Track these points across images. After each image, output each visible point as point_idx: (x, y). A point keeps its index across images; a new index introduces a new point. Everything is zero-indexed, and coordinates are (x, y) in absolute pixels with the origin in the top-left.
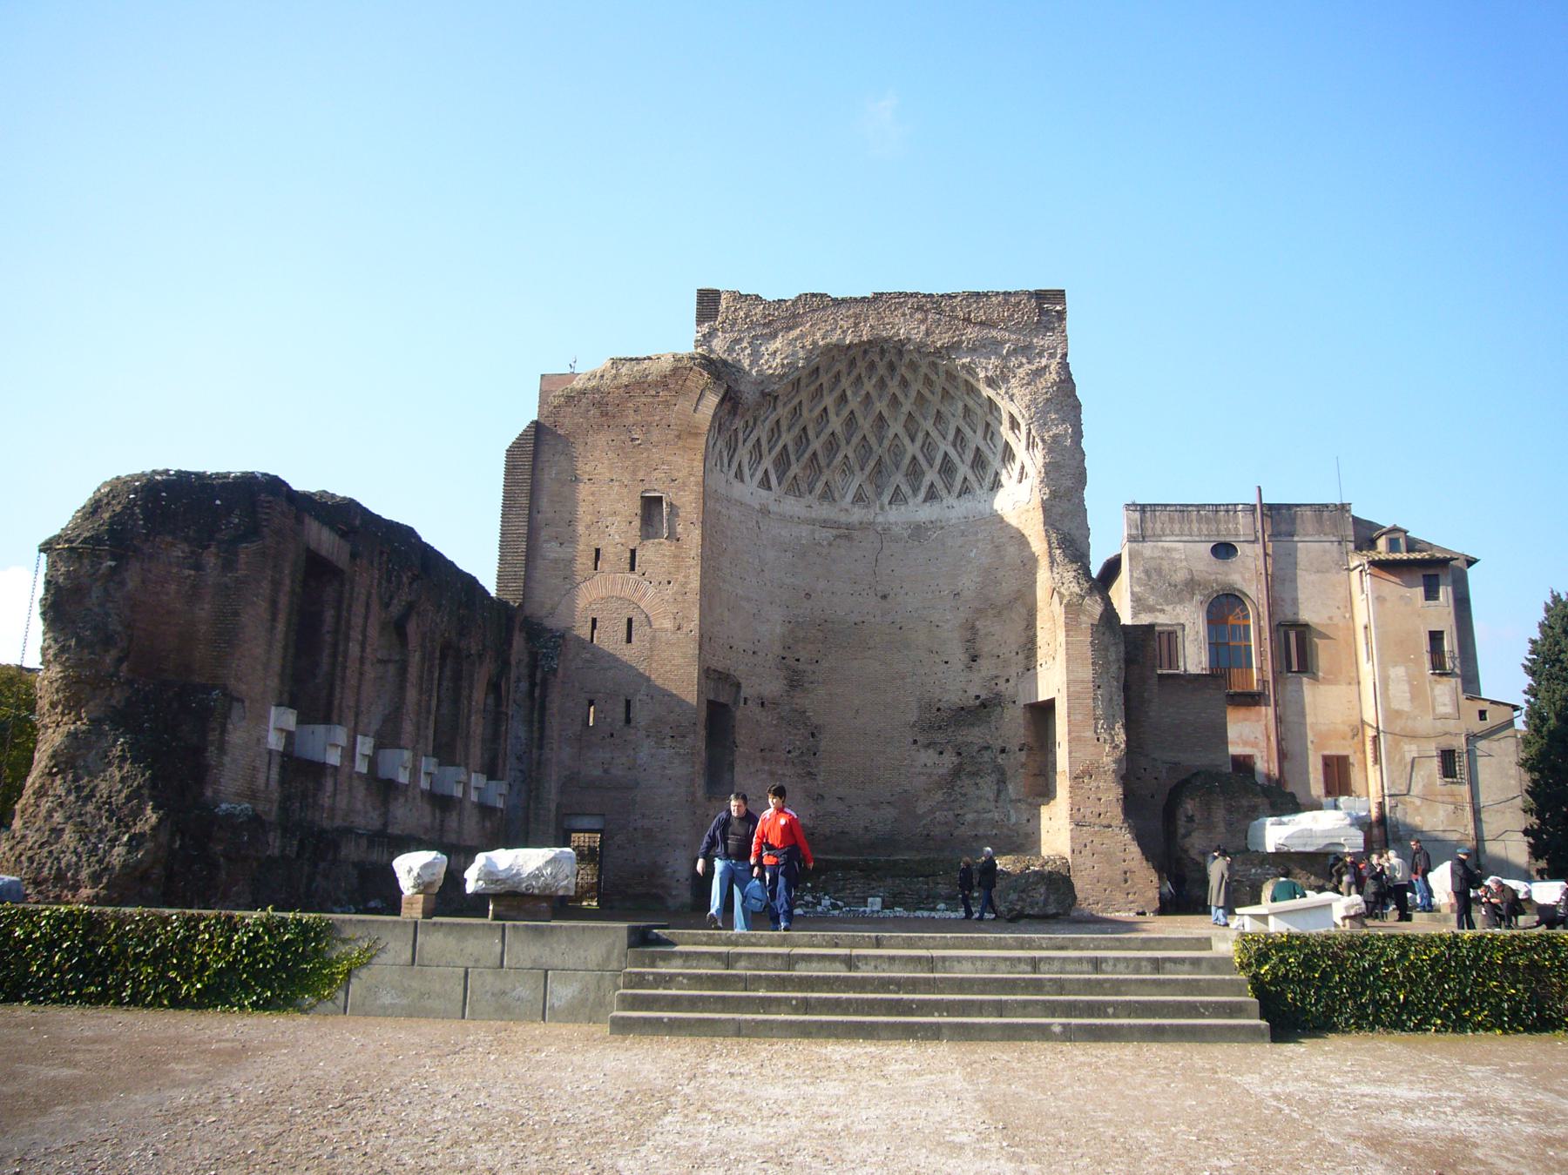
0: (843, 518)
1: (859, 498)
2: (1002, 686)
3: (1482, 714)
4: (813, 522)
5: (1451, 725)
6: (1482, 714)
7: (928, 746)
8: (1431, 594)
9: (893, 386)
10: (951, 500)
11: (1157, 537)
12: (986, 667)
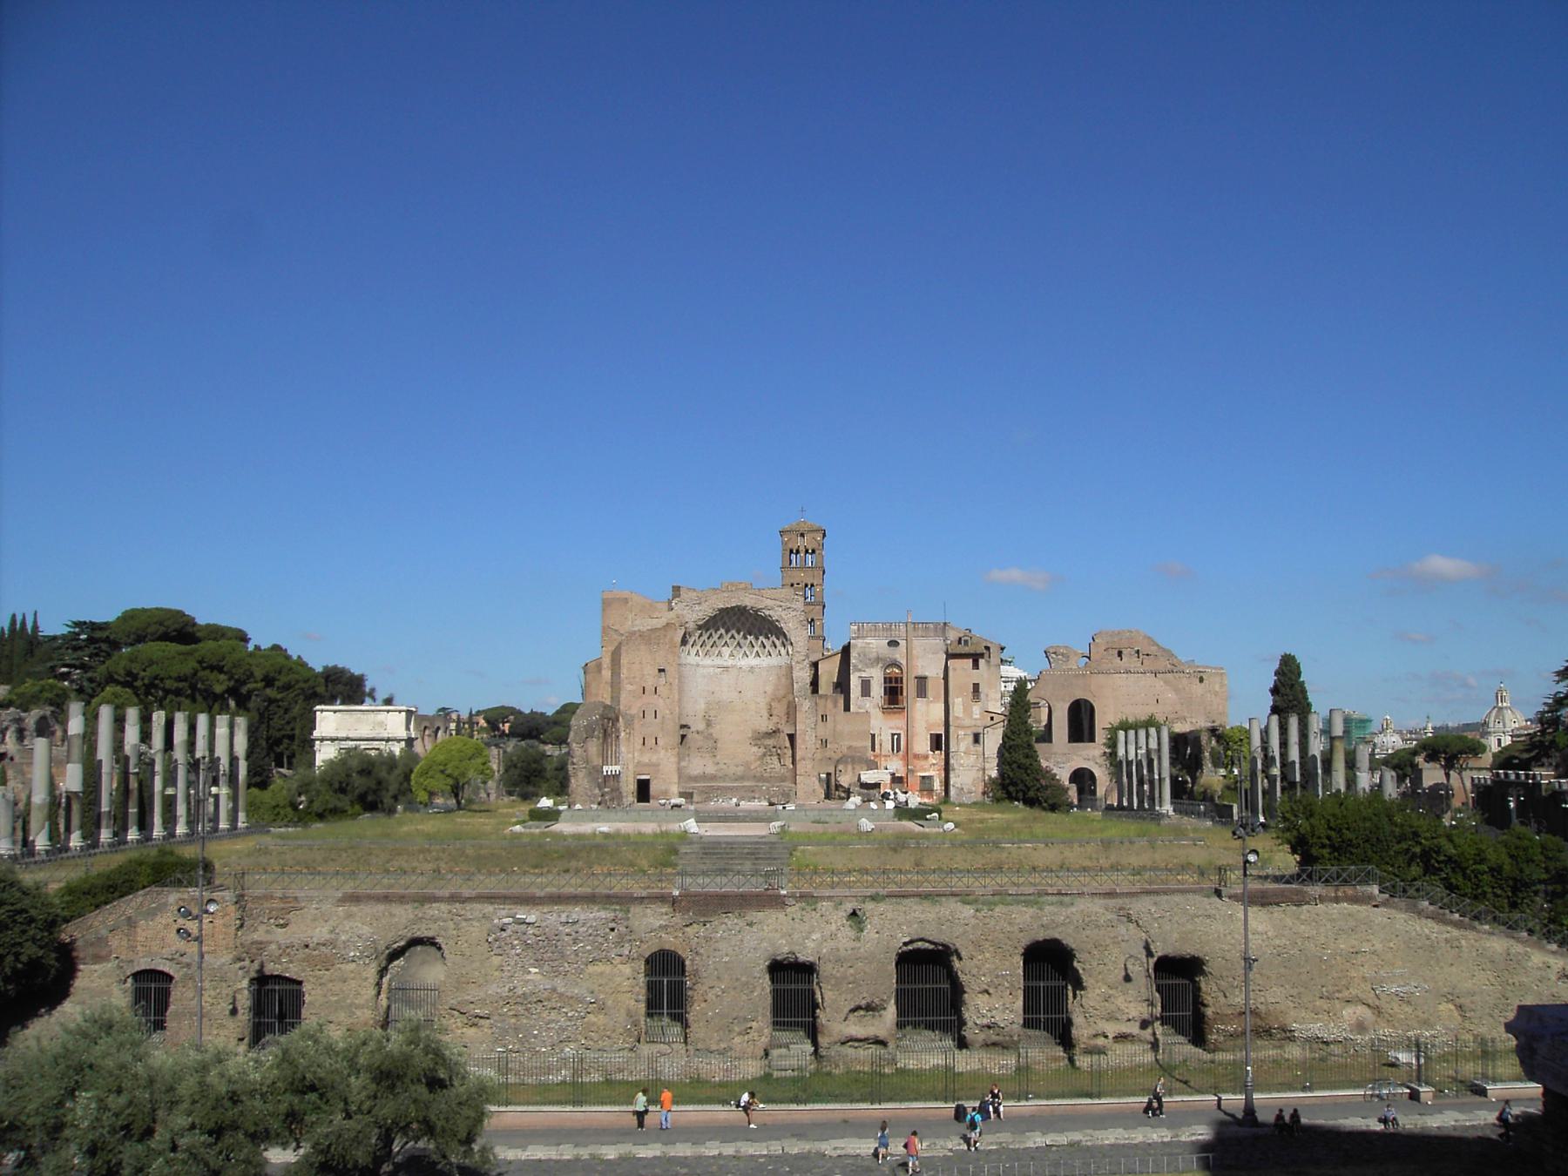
0: (725, 664)
1: (732, 655)
2: (779, 726)
3: (992, 719)
4: (713, 666)
5: (979, 723)
6: (992, 719)
7: (756, 745)
8: (976, 666)
9: (743, 618)
10: (763, 658)
11: (863, 637)
12: (775, 719)
